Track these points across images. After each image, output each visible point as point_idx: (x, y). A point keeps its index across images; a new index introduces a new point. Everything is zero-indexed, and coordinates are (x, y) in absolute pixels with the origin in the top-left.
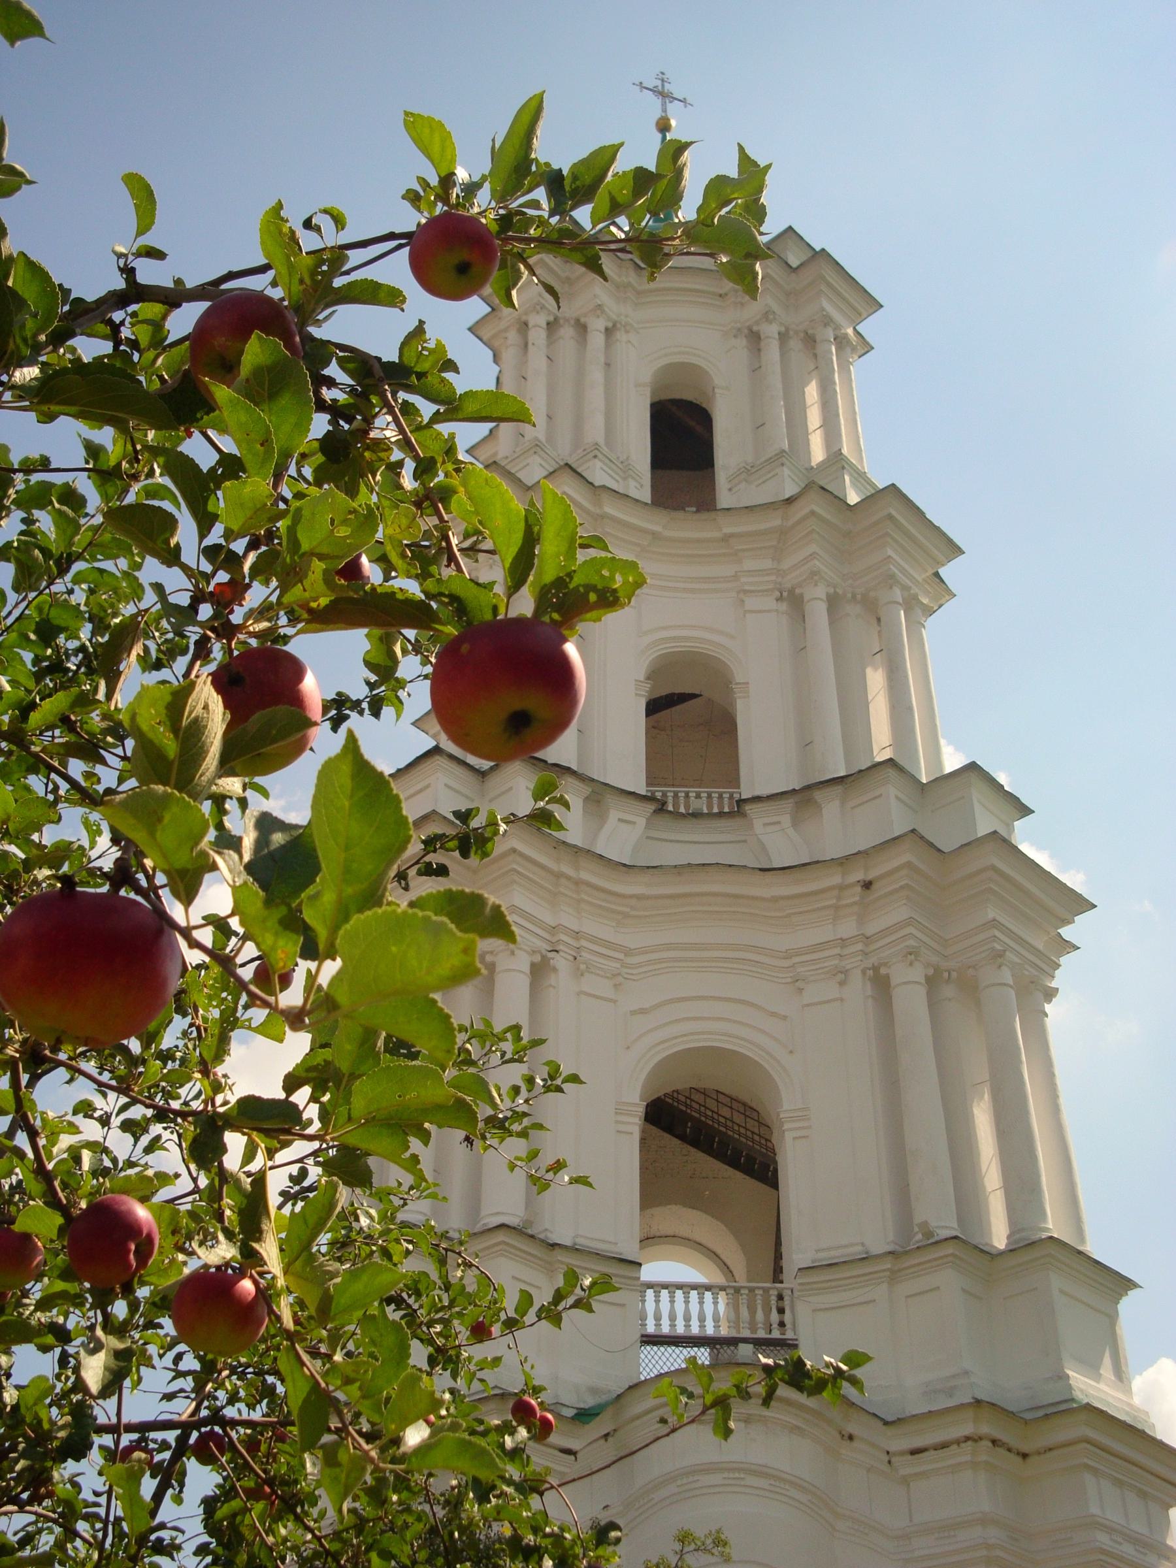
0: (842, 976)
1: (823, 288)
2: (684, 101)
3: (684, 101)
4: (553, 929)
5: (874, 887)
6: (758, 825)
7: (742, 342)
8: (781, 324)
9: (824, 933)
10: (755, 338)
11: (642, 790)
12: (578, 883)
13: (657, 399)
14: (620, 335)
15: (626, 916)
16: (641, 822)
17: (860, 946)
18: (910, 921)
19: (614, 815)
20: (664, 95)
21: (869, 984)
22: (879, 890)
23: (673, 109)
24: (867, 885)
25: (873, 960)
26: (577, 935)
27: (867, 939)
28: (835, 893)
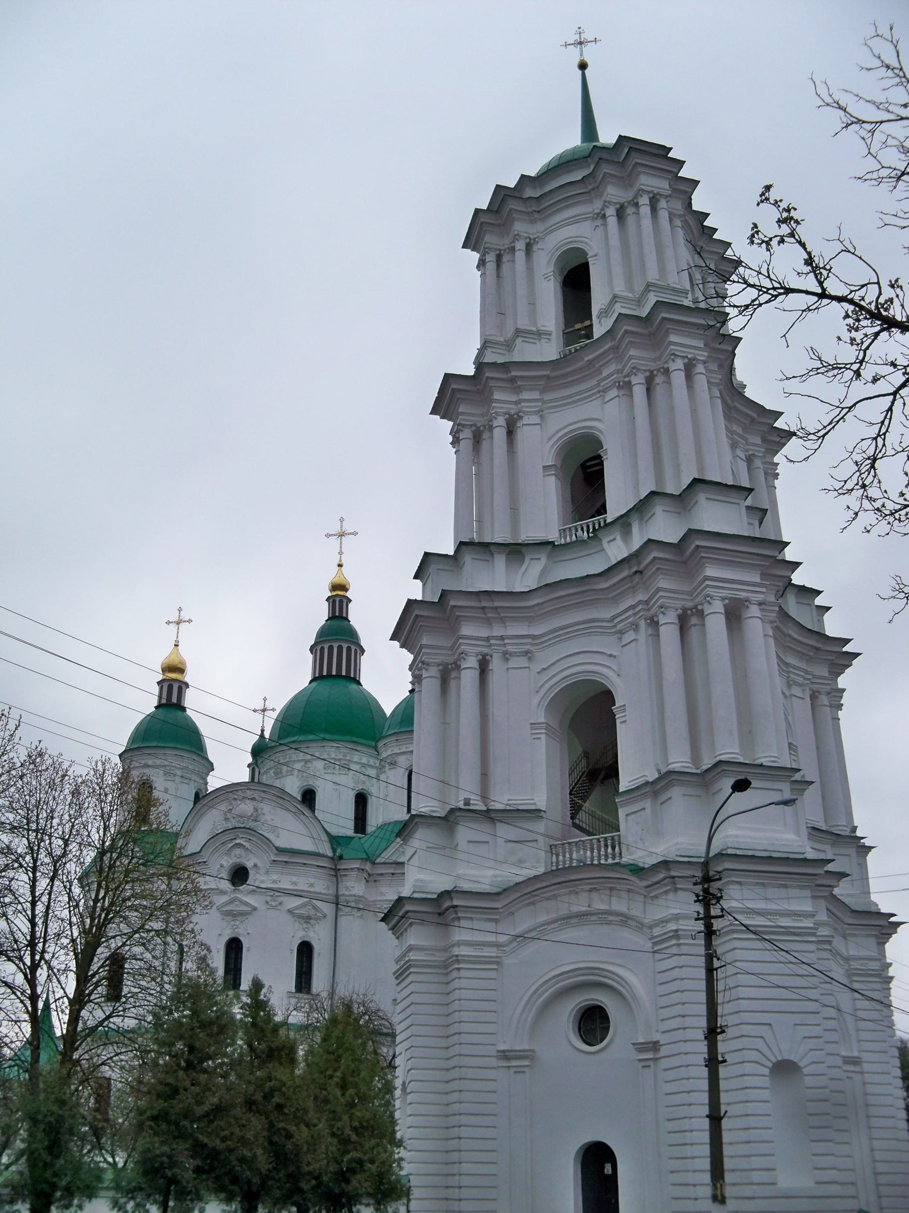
0: (635, 627)
1: (640, 169)
4: (488, 639)
5: (645, 572)
6: (605, 542)
7: (599, 222)
9: (630, 602)
12: (496, 608)
15: (533, 617)
22: (648, 574)
26: (502, 638)
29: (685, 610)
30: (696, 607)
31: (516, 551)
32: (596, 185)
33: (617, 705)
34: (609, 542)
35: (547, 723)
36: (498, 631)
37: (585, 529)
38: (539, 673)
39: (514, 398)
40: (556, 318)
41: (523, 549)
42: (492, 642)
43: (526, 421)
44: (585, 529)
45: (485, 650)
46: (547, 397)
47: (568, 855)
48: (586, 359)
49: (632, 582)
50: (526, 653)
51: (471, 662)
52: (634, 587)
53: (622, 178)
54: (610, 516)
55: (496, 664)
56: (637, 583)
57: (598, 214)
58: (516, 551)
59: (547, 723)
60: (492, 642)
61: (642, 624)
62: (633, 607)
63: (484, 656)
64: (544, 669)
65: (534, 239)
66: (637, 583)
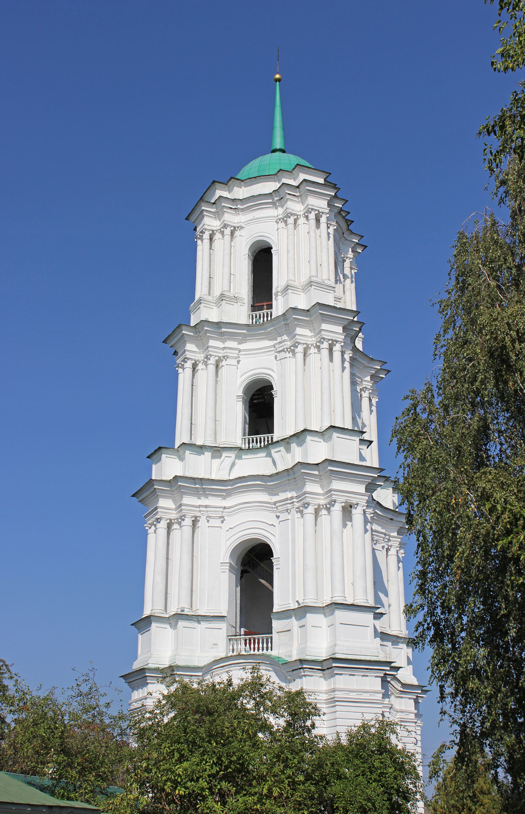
14: (237, 233)
16: (233, 456)
26: (206, 507)
31: (217, 451)
33: (274, 557)
35: (230, 563)
36: (204, 501)
38: (227, 531)
39: (221, 345)
40: (248, 275)
46: (242, 347)
50: (220, 517)
51: (188, 522)
54: (277, 435)
55: (202, 523)
58: (217, 451)
59: (230, 563)
60: (201, 509)
61: (294, 511)
63: (196, 517)
64: (230, 528)
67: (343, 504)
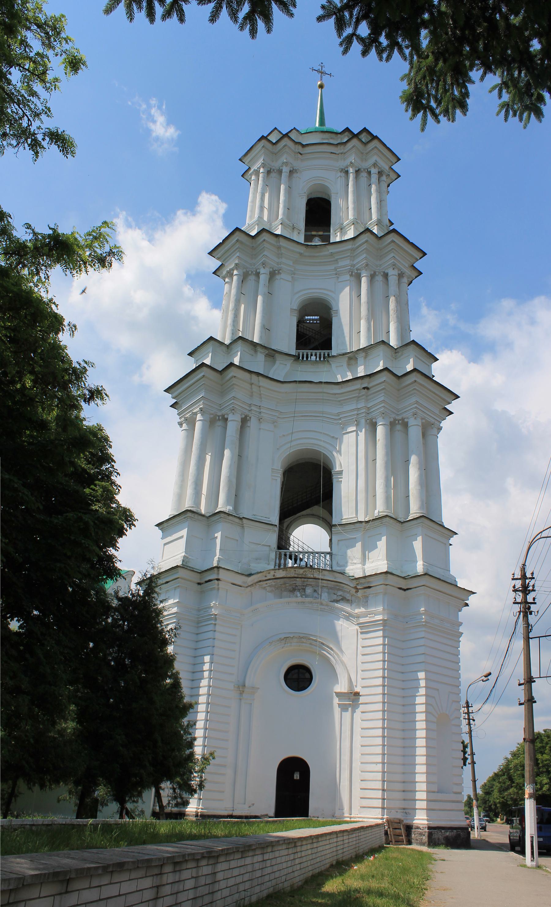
2: (330, 75)
3: (330, 75)
8: (356, 167)
9: (353, 406)
10: (347, 172)
11: (293, 352)
13: (310, 197)
17: (364, 411)
18: (383, 401)
19: (278, 362)
20: (322, 73)
21: (367, 426)
22: (372, 391)
23: (325, 77)
24: (367, 388)
25: (370, 417)
27: (369, 408)
28: (358, 391)
29: (395, 420)
30: (403, 419)
32: (345, 151)
34: (337, 367)
37: (318, 355)
41: (277, 355)
42: (253, 408)
43: (283, 276)
44: (318, 355)
45: (247, 413)
47: (282, 561)
48: (331, 251)
49: (359, 394)
52: (359, 397)
53: (362, 153)
55: (253, 423)
56: (363, 395)
57: (342, 170)
62: (358, 409)
64: (284, 436)
65: (296, 170)
66: (363, 395)
67: (424, 421)
